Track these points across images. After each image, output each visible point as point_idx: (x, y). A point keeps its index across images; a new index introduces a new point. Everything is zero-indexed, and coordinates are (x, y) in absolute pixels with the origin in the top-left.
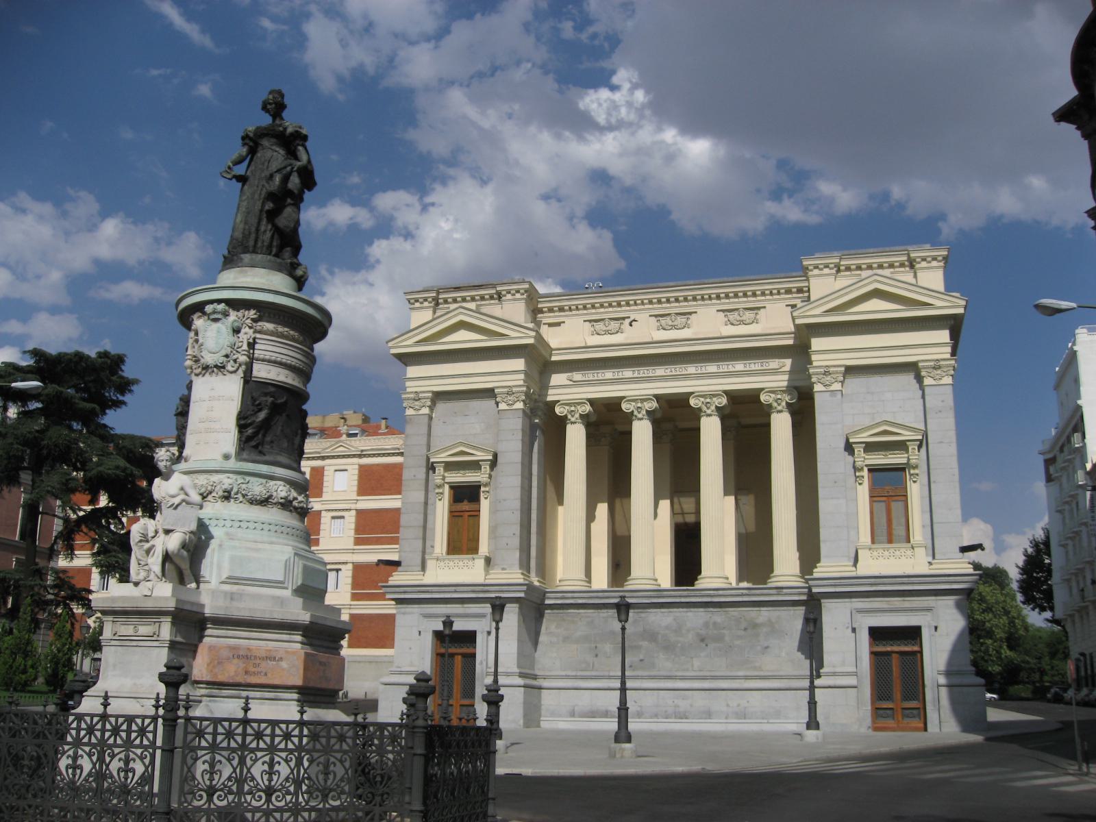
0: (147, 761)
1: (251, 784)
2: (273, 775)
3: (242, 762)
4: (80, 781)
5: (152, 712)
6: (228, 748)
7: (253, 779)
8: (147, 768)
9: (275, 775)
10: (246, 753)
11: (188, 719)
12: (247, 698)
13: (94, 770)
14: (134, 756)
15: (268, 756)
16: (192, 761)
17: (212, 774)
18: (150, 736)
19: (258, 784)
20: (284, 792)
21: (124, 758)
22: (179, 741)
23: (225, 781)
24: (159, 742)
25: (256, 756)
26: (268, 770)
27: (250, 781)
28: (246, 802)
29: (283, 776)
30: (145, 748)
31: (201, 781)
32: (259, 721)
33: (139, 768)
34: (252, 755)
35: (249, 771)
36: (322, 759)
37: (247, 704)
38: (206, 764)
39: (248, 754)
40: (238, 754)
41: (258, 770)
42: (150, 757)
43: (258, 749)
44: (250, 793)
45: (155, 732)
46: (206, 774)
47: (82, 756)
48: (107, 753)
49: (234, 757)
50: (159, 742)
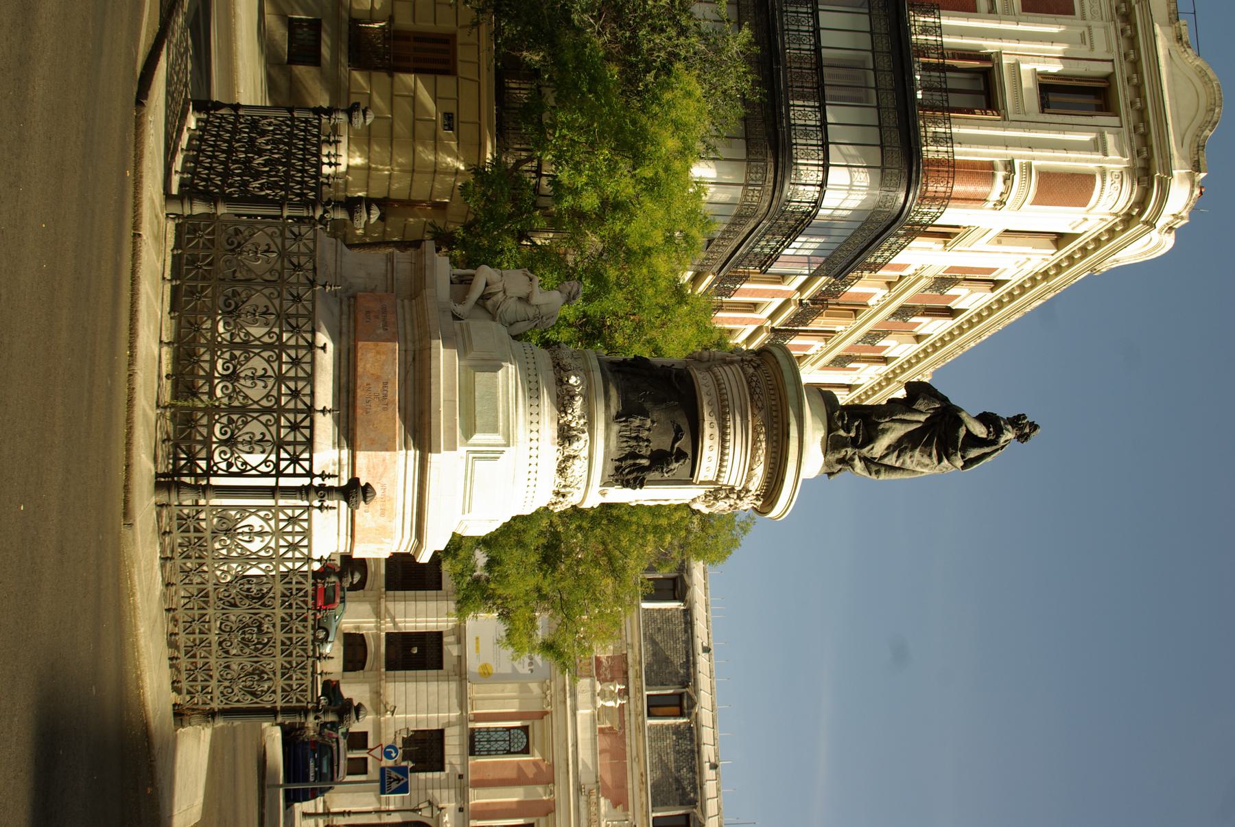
1: (240, 422)
3: (266, 410)
7: (245, 423)
17: (253, 378)
27: (243, 421)
28: (220, 417)
32: (311, 427)
34: (273, 420)
35: (254, 418)
39: (273, 416)
40: (273, 406)
44: (231, 421)
46: (252, 373)
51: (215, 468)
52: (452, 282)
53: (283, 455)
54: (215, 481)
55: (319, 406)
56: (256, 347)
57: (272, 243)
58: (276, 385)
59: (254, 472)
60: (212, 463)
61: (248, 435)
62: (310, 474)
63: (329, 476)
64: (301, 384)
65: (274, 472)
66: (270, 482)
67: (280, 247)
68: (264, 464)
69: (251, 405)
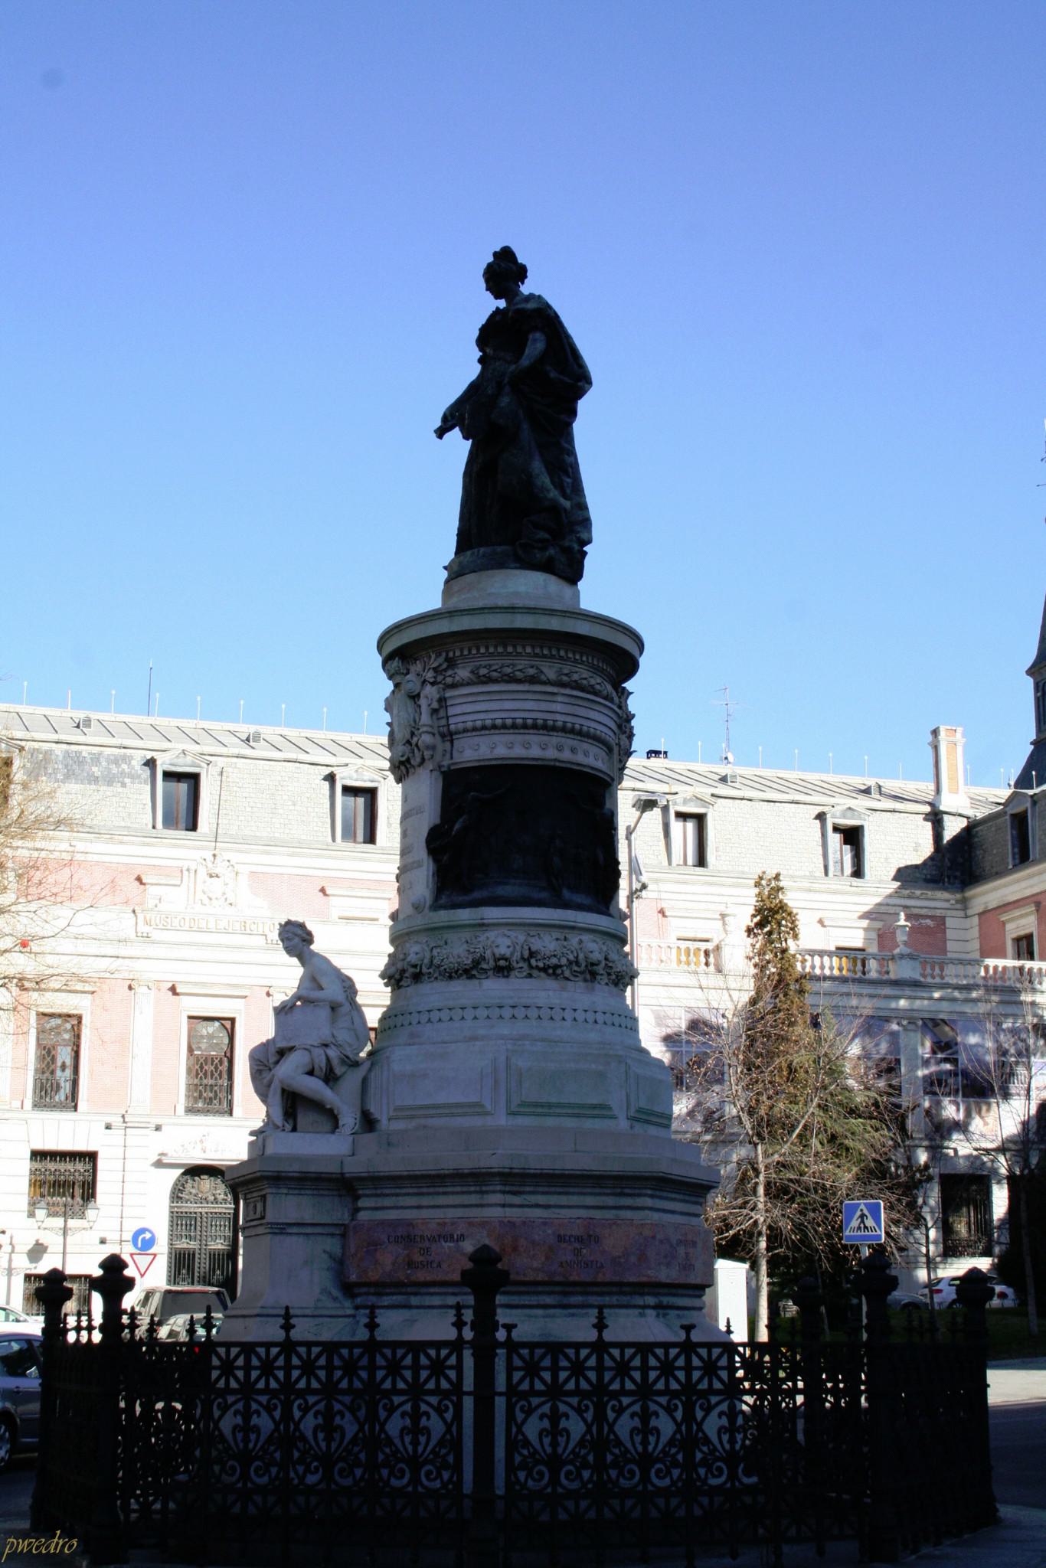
0: (449, 1416)
1: (617, 1451)
2: (420, 1436)
4: (566, 1455)
5: (451, 1334)
6: (577, 1392)
8: (449, 1426)
9: (562, 1436)
10: (605, 1399)
11: (512, 1346)
12: (601, 1308)
13: (448, 1437)
14: (341, 1407)
15: (323, 1404)
16: (614, 1415)
18: (452, 1374)
19: (715, 1449)
20: (668, 1463)
21: (242, 1409)
22: (501, 1383)
23: (575, 1447)
24: (468, 1384)
25: (530, 1403)
26: (727, 1425)
29: (664, 1440)
30: (445, 1395)
31: (629, 1445)
32: (622, 1346)
33: (435, 1425)
34: (523, 1403)
36: (724, 1407)
37: (601, 1318)
38: (636, 1419)
41: (624, 1426)
42: (683, 1410)
43: (623, 1392)
45: (459, 1367)
47: (567, 1416)
48: (381, 1405)
49: (587, 1407)
50: (468, 1384)
51: (590, 1486)
52: (294, 1129)
53: (660, 1385)
54: (468, 1487)
55: (592, 1336)
56: (287, 1427)
57: (233, 1410)
58: (655, 1398)
59: (454, 1429)
60: (443, 1491)
61: (237, 1434)
62: (457, 1345)
63: (459, 1315)
64: (380, 1361)
65: (455, 1398)
66: (468, 1403)
67: (543, 1399)
68: (585, 1415)
69: (452, 1435)
